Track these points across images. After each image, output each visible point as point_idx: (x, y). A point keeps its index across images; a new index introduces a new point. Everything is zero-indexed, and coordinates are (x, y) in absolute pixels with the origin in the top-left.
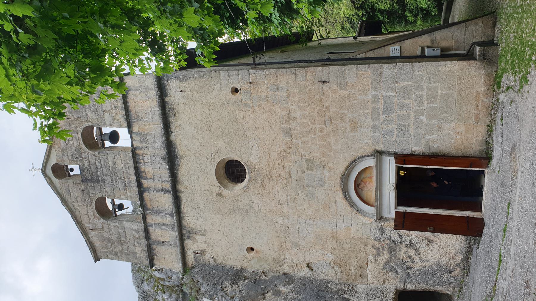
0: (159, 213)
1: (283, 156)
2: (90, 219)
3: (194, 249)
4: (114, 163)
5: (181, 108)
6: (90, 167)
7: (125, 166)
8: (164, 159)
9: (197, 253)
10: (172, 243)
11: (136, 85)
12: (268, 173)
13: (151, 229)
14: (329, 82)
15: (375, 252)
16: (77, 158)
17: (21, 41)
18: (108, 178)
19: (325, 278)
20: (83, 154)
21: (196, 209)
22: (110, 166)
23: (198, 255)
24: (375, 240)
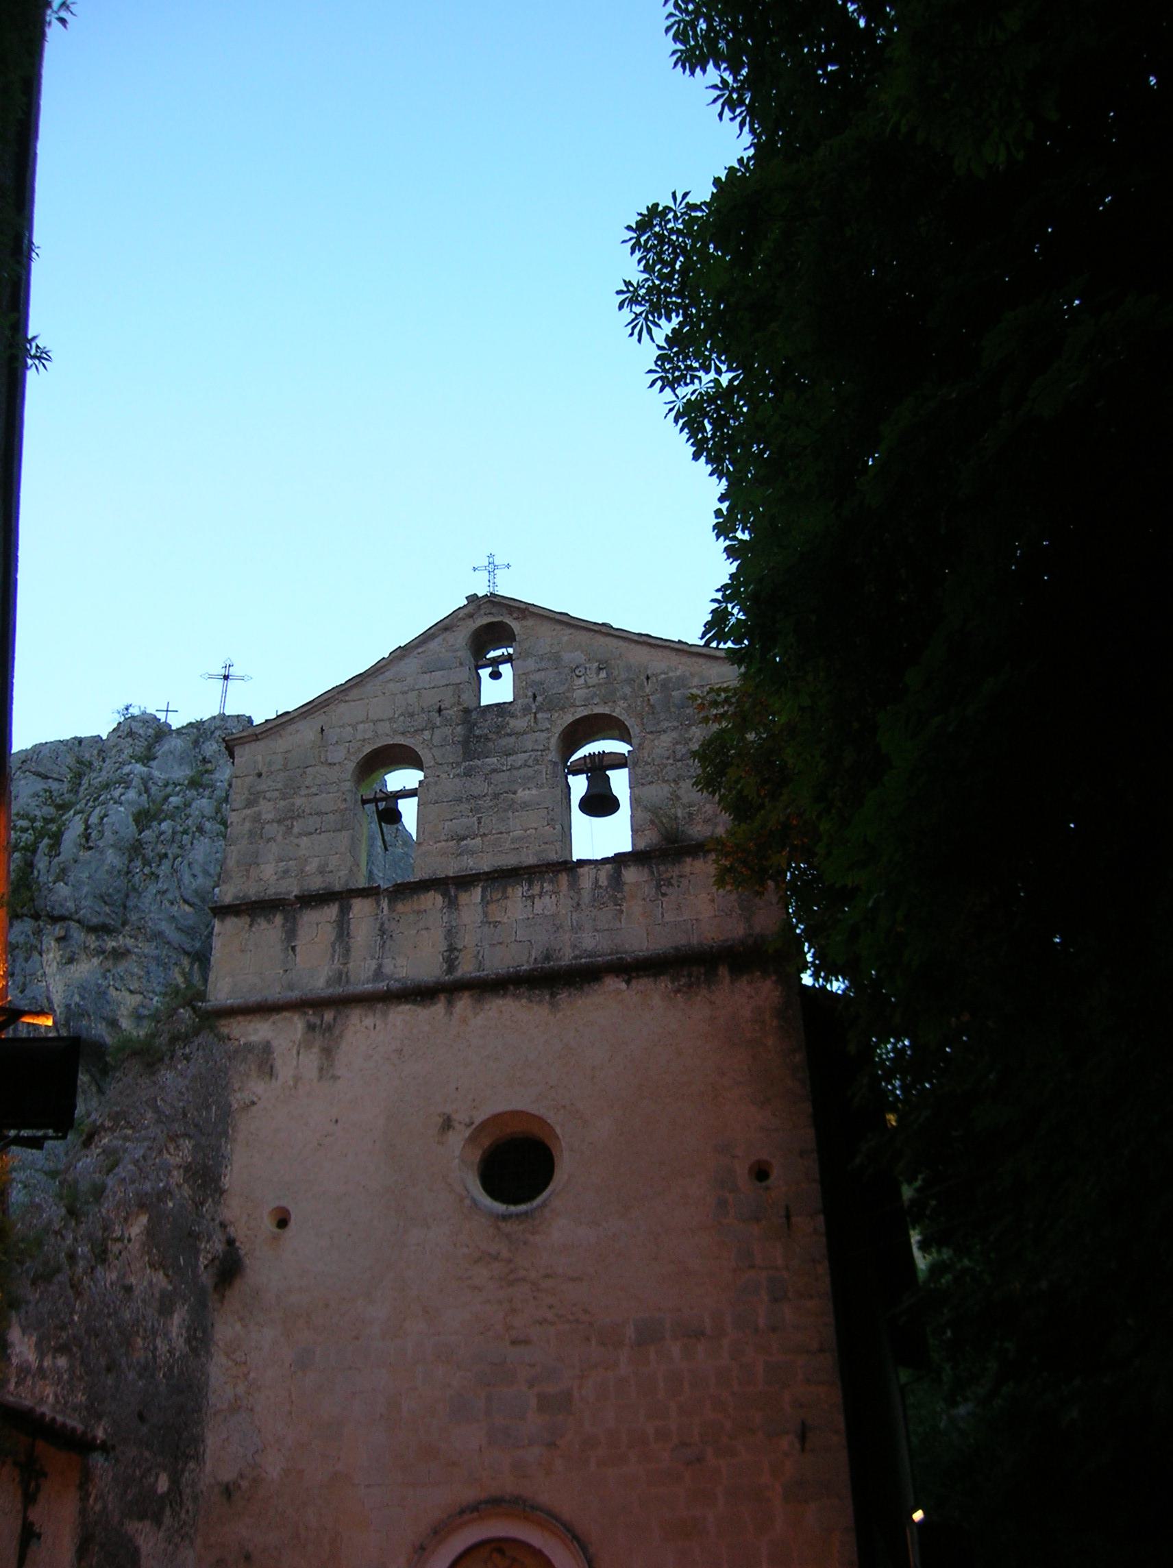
1: (577, 1321)
2: (355, 728)
3: (275, 1043)
4: (525, 806)
6: (509, 735)
7: (521, 839)
8: (547, 958)
12: (522, 1273)
13: (332, 911)
14: (803, 1450)
16: (535, 697)
18: (479, 786)
19: (208, 1451)
21: (399, 1051)
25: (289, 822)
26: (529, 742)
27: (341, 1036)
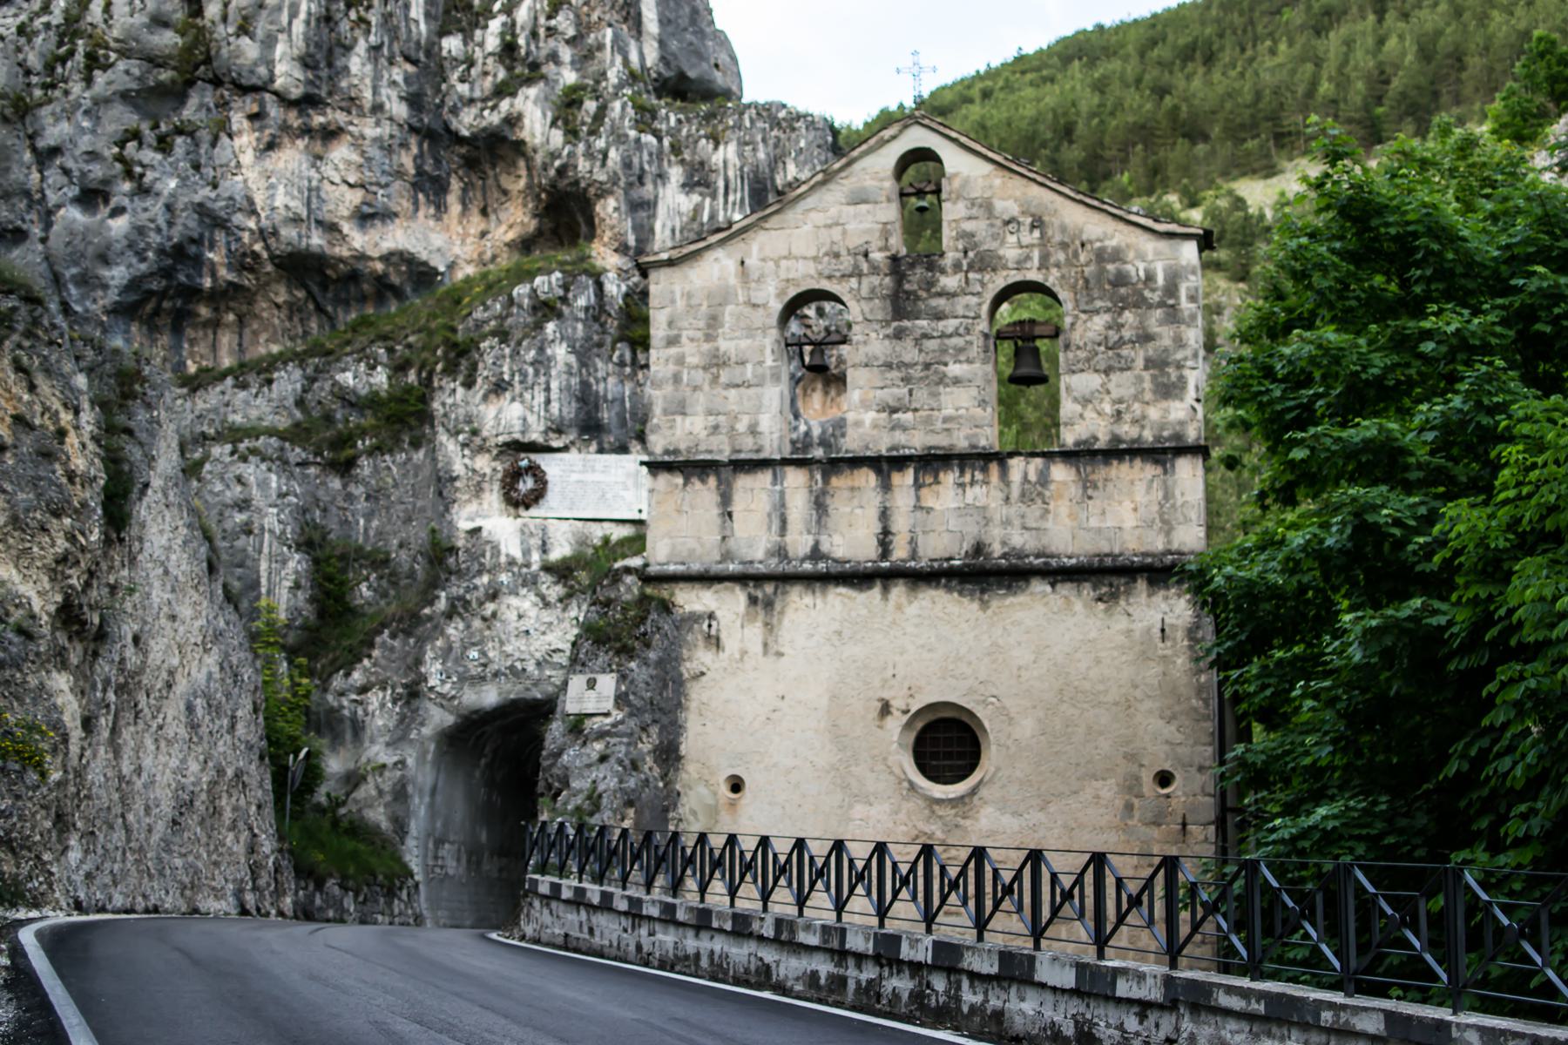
3: (718, 614)
4: (957, 381)
5: (1120, 623)
6: (940, 295)
10: (731, 543)
11: (1177, 493)
13: (765, 478)
17: (1329, 1031)
18: (909, 352)
20: (978, 276)
21: (839, 633)
22: (946, 364)
23: (705, 626)
25: (714, 370)
26: (960, 304)
27: (782, 613)
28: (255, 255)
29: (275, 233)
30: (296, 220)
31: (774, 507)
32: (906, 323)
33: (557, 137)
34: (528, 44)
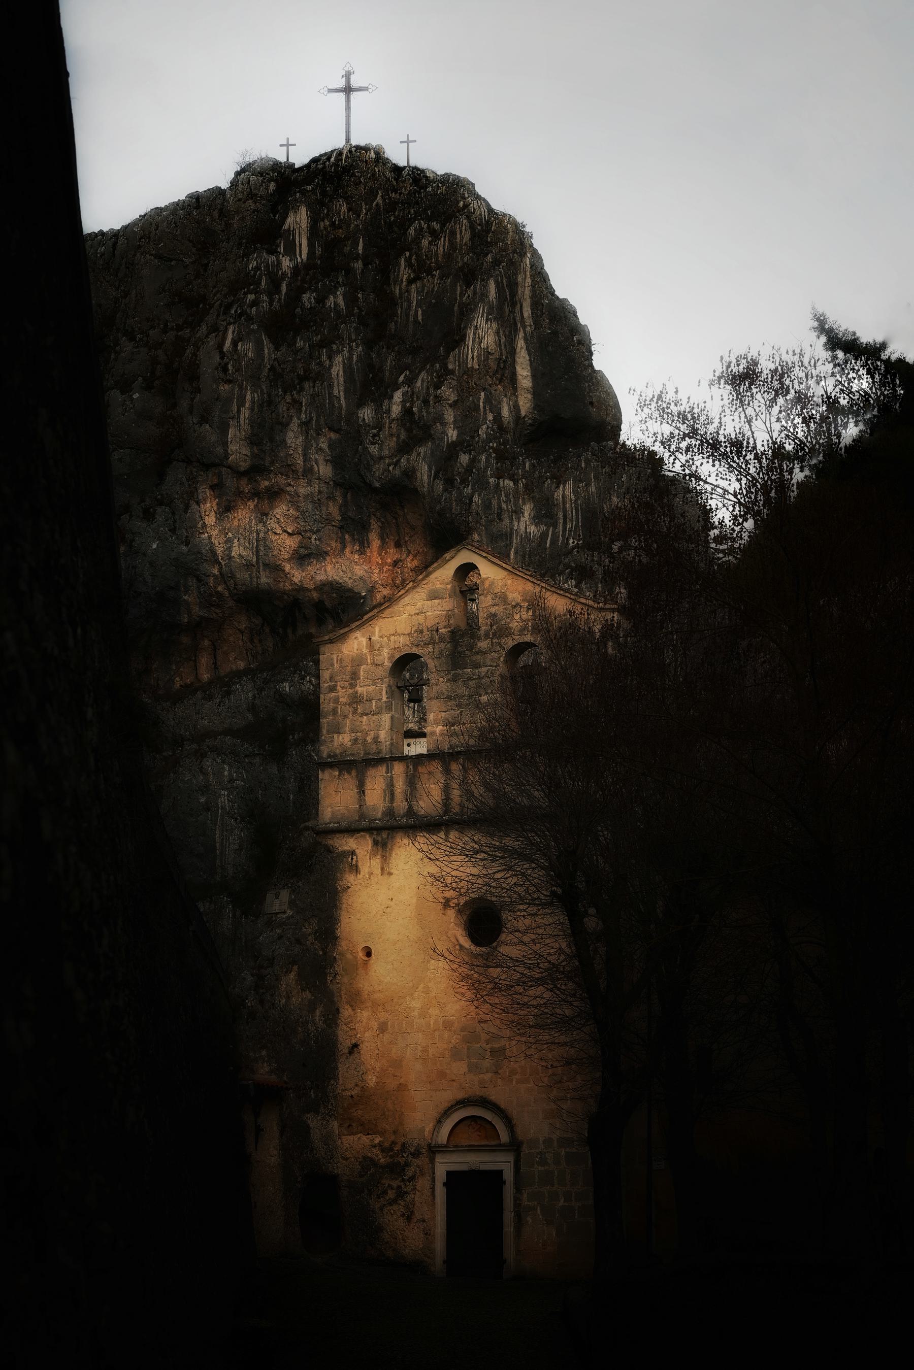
0: (411, 789)
3: (357, 851)
6: (477, 653)
9: (352, 859)
13: (382, 769)
15: (387, 1144)
19: (340, 1073)
23: (350, 860)
24: (403, 1145)
25: (355, 705)
27: (391, 849)
28: (220, 595)
29: (233, 577)
30: (248, 566)
31: (387, 786)
32: (459, 671)
33: (440, 486)
34: (420, 411)
